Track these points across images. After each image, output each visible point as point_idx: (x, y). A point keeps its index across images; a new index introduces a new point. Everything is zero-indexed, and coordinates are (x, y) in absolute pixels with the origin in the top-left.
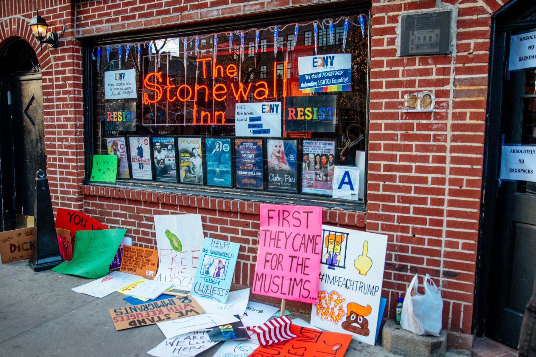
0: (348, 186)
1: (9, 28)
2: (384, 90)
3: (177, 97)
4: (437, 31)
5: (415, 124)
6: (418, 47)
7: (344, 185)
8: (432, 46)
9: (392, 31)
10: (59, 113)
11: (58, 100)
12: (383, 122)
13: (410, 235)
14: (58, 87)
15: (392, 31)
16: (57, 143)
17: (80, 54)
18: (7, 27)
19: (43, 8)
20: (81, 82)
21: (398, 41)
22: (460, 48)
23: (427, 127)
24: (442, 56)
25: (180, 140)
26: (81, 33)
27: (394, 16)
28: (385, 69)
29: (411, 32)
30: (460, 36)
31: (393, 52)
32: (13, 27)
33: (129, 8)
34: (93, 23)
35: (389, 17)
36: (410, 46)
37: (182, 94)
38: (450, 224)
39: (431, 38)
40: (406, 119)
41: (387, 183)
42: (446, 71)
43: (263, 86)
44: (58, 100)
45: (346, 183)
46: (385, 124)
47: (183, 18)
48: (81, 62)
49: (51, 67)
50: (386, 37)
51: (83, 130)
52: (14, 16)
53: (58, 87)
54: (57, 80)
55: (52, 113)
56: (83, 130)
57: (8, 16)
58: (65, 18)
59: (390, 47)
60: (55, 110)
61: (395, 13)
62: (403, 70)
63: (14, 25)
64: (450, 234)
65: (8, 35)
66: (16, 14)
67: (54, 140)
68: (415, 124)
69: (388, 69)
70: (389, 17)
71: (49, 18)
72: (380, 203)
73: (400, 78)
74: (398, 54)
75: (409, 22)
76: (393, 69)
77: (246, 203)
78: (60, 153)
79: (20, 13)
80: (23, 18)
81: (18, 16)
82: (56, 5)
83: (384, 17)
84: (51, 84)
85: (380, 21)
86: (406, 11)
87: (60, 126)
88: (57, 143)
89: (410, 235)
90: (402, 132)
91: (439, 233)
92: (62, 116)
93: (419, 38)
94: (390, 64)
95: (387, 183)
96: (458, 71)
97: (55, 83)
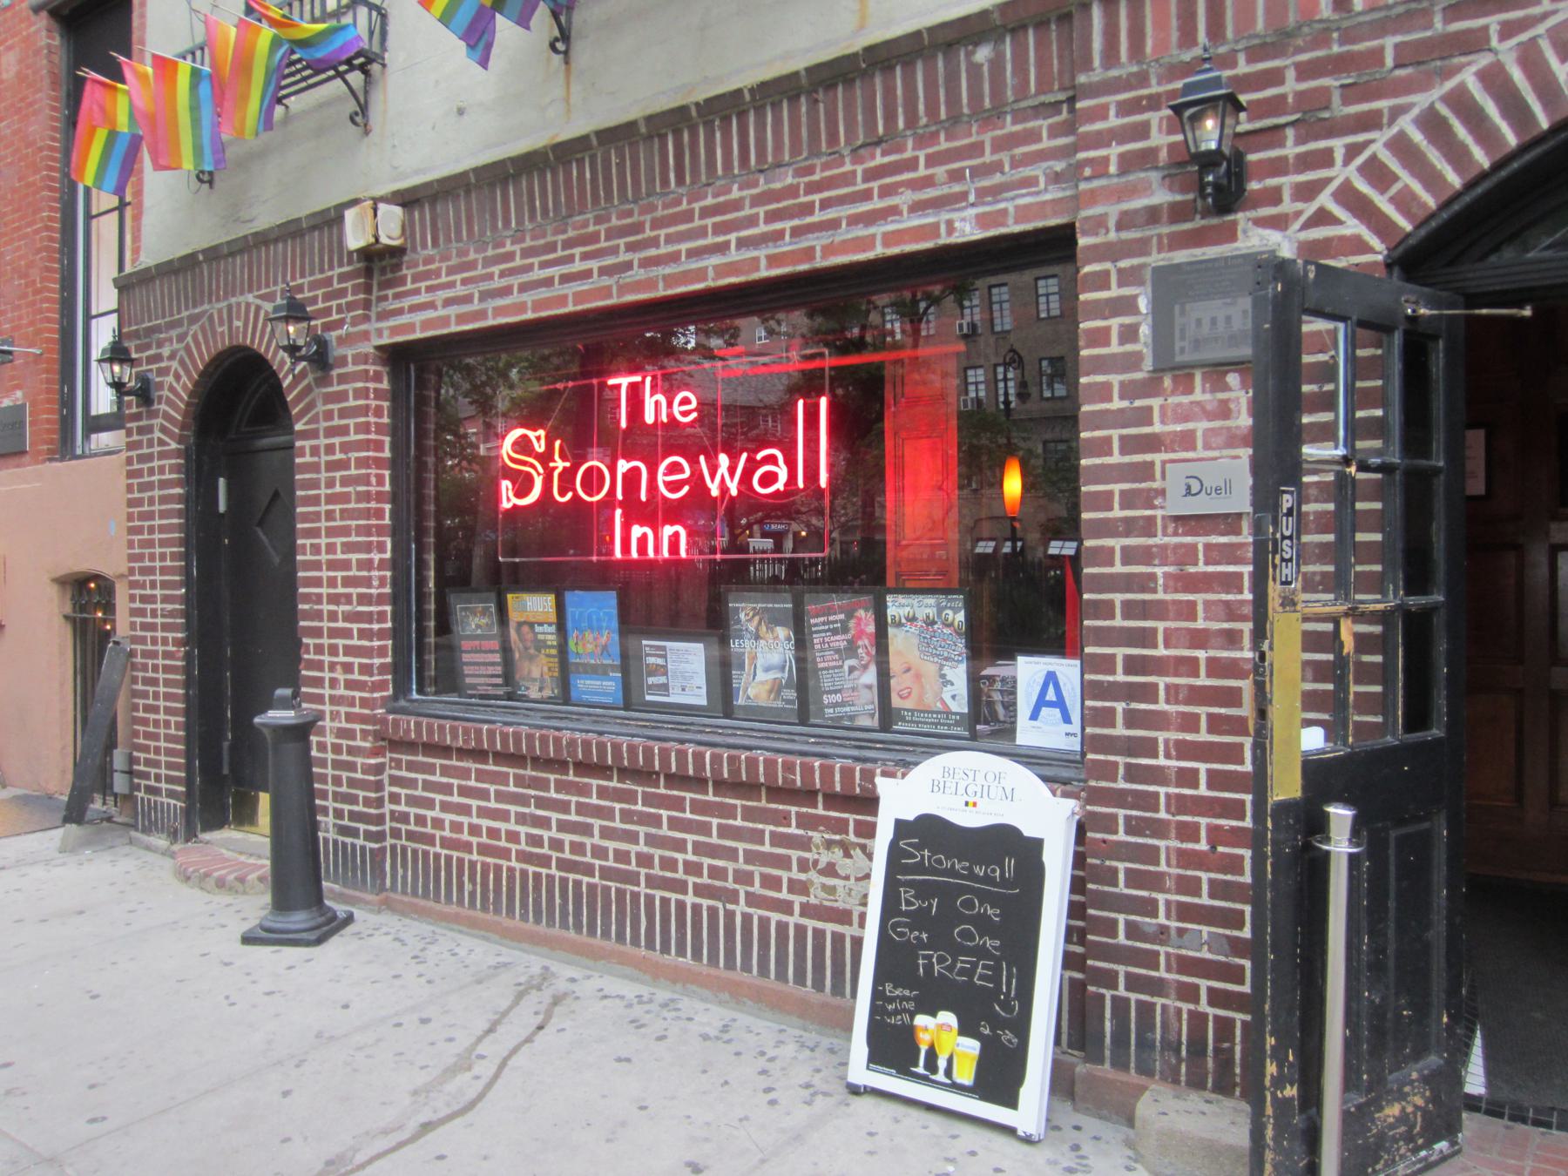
0: (1057, 712)
1: (225, 328)
2: (1116, 458)
3: (574, 490)
5: (1200, 547)
6: (1197, 344)
7: (1045, 711)
8: (1233, 340)
9: (1128, 306)
10: (331, 532)
11: (331, 499)
12: (1117, 543)
13: (1203, 846)
14: (332, 466)
15: (1128, 306)
16: (326, 607)
17: (385, 385)
18: (221, 323)
19: (303, 276)
20: (387, 454)
21: (1145, 330)
23: (1146, 555)
25: (571, 597)
26: (386, 333)
27: (1132, 267)
28: (1117, 404)
29: (1177, 308)
33: (496, 269)
34: (414, 309)
35: (1120, 271)
36: (1178, 345)
37: (589, 487)
39: (1228, 319)
40: (1175, 534)
41: (1134, 705)
43: (771, 459)
44: (331, 499)
45: (1051, 704)
46: (1124, 549)
47: (623, 289)
48: (386, 404)
49: (315, 420)
50: (1115, 323)
51: (389, 574)
52: (241, 299)
53: (332, 466)
54: (330, 449)
56: (389, 574)
57: (226, 298)
58: (350, 298)
59: (1129, 347)
60: (323, 524)
61: (1135, 261)
62: (1162, 407)
63: (238, 319)
65: (224, 343)
66: (242, 293)
68: (1200, 547)
69: (1125, 404)
70: (1120, 271)
71: (314, 300)
72: (1119, 759)
73: (1157, 428)
74: (1148, 364)
76: (1138, 403)
77: (817, 764)
78: (334, 633)
79: (250, 291)
80: (259, 302)
81: (250, 298)
82: (331, 268)
83: (1107, 273)
84: (316, 459)
85: (1102, 281)
86: (1162, 255)
87: (332, 565)
88: (326, 607)
89: (1203, 846)
90: (1166, 569)
93: (1199, 322)
94: (1128, 391)
95: (1134, 705)
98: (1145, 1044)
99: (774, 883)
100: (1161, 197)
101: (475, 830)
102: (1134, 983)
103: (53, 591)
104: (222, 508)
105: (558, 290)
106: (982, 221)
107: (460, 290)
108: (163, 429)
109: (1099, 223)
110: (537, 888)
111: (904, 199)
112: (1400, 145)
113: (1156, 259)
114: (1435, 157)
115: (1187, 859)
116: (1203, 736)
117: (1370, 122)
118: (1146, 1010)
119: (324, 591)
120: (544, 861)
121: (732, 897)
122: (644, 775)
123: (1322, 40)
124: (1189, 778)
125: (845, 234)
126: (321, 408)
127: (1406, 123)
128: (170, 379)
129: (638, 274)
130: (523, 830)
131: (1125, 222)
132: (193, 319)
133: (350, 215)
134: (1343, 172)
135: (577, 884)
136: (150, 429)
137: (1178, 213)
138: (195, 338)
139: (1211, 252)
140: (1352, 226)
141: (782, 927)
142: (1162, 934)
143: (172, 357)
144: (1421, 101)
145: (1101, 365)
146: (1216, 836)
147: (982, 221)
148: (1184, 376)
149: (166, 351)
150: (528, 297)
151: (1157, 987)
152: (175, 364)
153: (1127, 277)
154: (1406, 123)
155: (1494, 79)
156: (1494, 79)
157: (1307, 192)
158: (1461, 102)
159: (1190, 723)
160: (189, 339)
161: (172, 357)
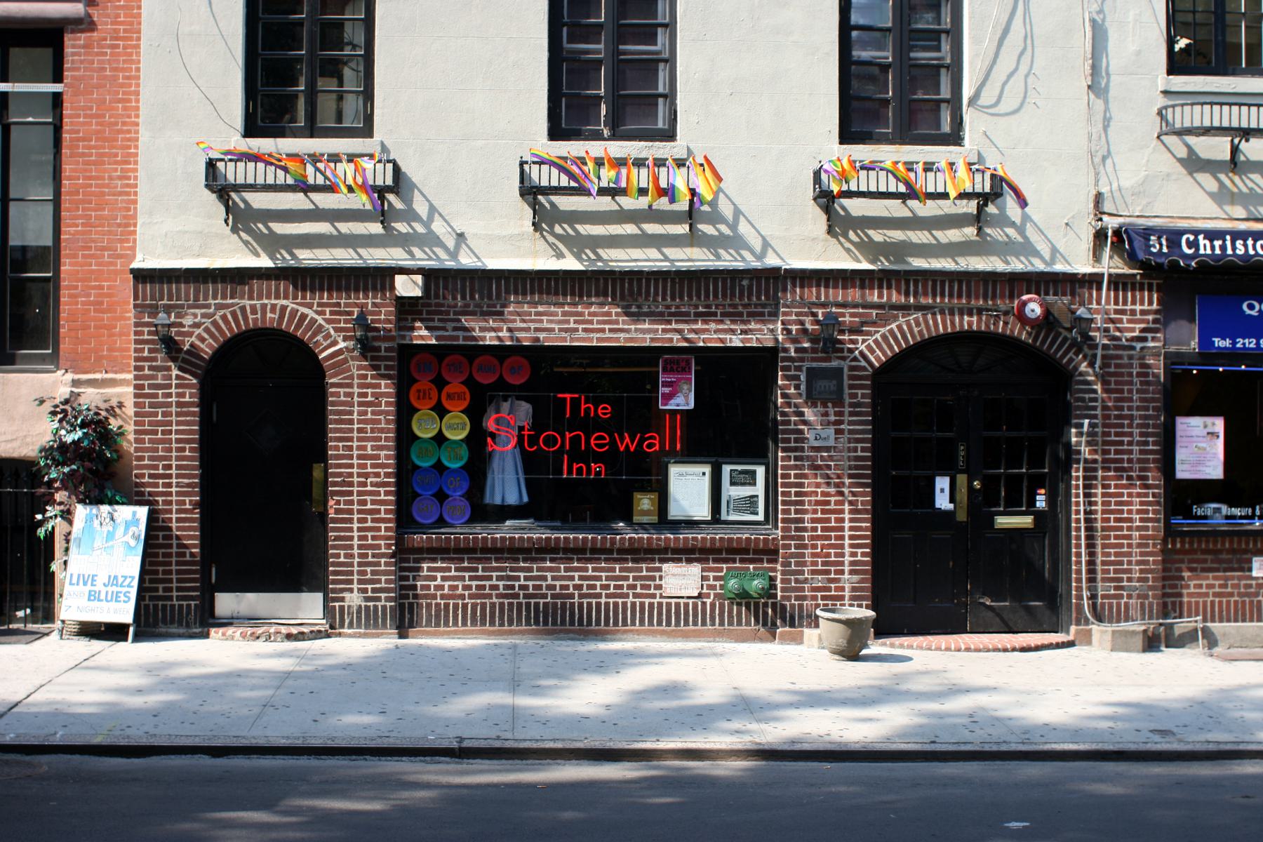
4: (834, 382)
6: (820, 393)
21: (803, 387)
24: (839, 402)
30: (851, 387)
32: (269, 315)
38: (851, 538)
42: (840, 414)
54: (360, 395)
55: (351, 439)
64: (852, 546)
67: (351, 475)
75: (810, 371)
88: (356, 479)
91: (842, 547)
92: (369, 444)
96: (851, 414)
97: (356, 399)
98: (801, 617)
99: (649, 587)
102: (797, 598)
104: (215, 418)
106: (742, 341)
110: (511, 610)
112: (876, 341)
114: (885, 347)
115: (814, 555)
116: (819, 515)
117: (869, 333)
118: (801, 606)
119: (355, 470)
120: (516, 596)
121: (627, 596)
124: (815, 529)
127: (878, 336)
128: (193, 339)
129: (581, 334)
130: (501, 583)
133: (400, 280)
135: (537, 604)
138: (224, 317)
139: (824, 364)
140: (863, 363)
142: (806, 580)
143: (197, 325)
144: (883, 330)
146: (823, 547)
147: (742, 341)
151: (804, 598)
152: (198, 331)
154: (878, 336)
156: (899, 327)
158: (891, 331)
159: (815, 512)
160: (217, 317)
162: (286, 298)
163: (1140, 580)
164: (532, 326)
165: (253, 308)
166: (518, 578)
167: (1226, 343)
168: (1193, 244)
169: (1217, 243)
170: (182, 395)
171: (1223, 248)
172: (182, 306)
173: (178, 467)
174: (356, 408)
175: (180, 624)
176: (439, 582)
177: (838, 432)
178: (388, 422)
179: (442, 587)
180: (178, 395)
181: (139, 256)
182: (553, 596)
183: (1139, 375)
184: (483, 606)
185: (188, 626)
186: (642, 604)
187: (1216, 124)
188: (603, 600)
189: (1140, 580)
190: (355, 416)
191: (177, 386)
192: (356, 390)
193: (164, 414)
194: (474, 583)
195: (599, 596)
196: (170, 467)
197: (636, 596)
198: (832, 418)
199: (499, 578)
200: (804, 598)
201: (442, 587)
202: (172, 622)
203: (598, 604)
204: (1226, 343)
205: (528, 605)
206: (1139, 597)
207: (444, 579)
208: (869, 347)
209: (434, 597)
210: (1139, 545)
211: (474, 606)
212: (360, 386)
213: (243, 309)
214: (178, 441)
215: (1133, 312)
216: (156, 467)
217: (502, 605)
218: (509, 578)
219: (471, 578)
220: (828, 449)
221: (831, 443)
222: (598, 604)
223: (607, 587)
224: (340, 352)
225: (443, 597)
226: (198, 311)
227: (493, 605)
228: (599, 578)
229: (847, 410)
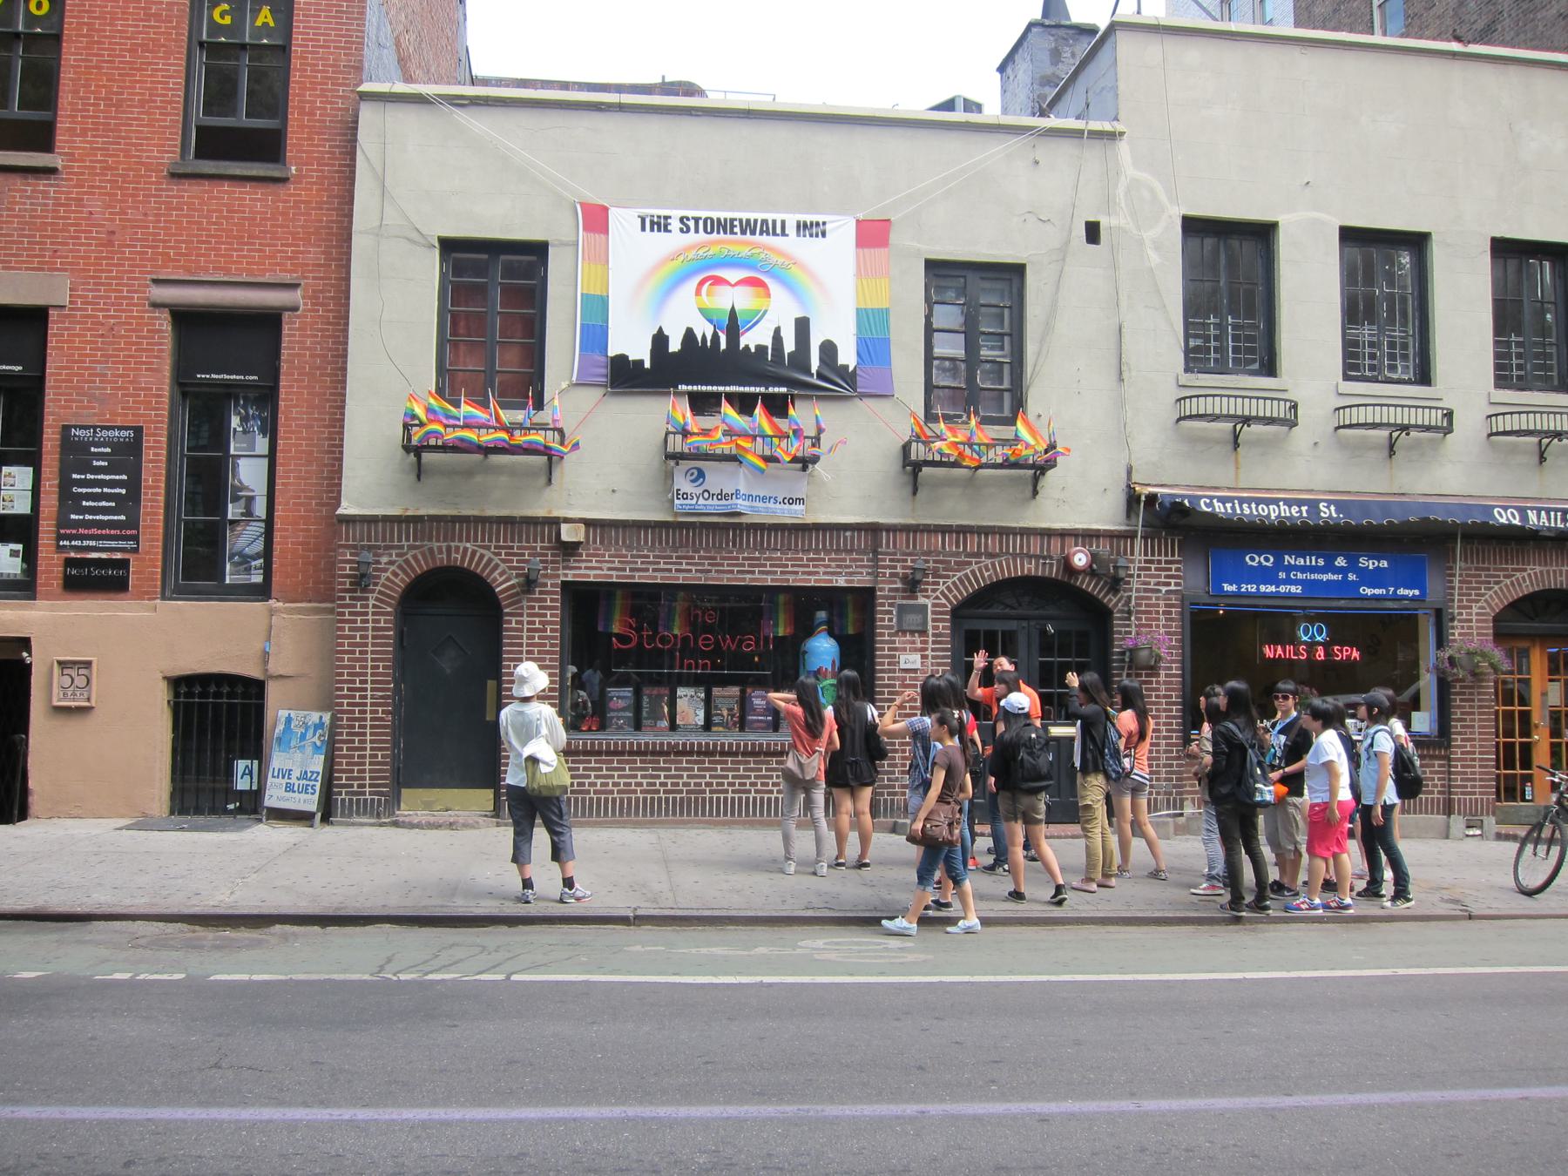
15: (890, 612)
22: (935, 628)
31: (890, 627)
100: (899, 585)
101: (615, 784)
103: (163, 686)
105: (674, 574)
107: (617, 565)
108: (377, 599)
109: (882, 589)
111: (822, 570)
113: (899, 602)
117: (948, 577)
122: (708, 753)
123: (938, 554)
125: (800, 576)
126: (525, 603)
131: (891, 590)
132: (411, 547)
133: (564, 527)
134: (941, 587)
136: (367, 599)
137: (904, 590)
138: (415, 557)
141: (769, 799)
143: (391, 563)
145: (883, 627)
148: (904, 632)
149: (384, 559)
150: (658, 574)
151: (895, 794)
152: (392, 568)
153: (891, 605)
155: (973, 572)
156: (973, 572)
157: (934, 591)
161: (391, 563)
162: (468, 540)
163: (1166, 780)
164: (674, 567)
165: (440, 549)
166: (659, 777)
167: (1234, 588)
168: (1210, 505)
169: (1229, 505)
170: (378, 621)
171: (1233, 508)
172: (379, 547)
173: (373, 682)
174: (525, 634)
175: (372, 816)
176: (592, 779)
177: (923, 657)
178: (552, 645)
179: (594, 784)
180: (374, 621)
181: (344, 503)
182: (688, 792)
183: (1164, 613)
184: (629, 800)
185: (378, 816)
186: (762, 799)
187: (1225, 412)
188: (730, 795)
189: (1166, 780)
190: (525, 641)
191: (374, 614)
192: (525, 619)
193: (362, 637)
194: (622, 781)
195: (726, 791)
196: (365, 682)
197: (757, 791)
198: (919, 645)
199: (643, 777)
200: (895, 794)
201: (594, 784)
202: (365, 813)
203: (726, 799)
204: (1234, 588)
205: (667, 800)
206: (1166, 793)
207: (597, 777)
208: (948, 588)
209: (588, 792)
210: (1166, 752)
211: (622, 800)
212: (529, 615)
213: (431, 550)
214: (373, 660)
215: (1159, 562)
216: (354, 682)
217: (645, 799)
218: (652, 777)
219: (620, 777)
220: (915, 671)
221: (918, 666)
222: (726, 799)
223: (733, 784)
224: (513, 587)
225: (596, 792)
226: (394, 552)
227: (637, 799)
228: (727, 777)
229: (931, 639)
